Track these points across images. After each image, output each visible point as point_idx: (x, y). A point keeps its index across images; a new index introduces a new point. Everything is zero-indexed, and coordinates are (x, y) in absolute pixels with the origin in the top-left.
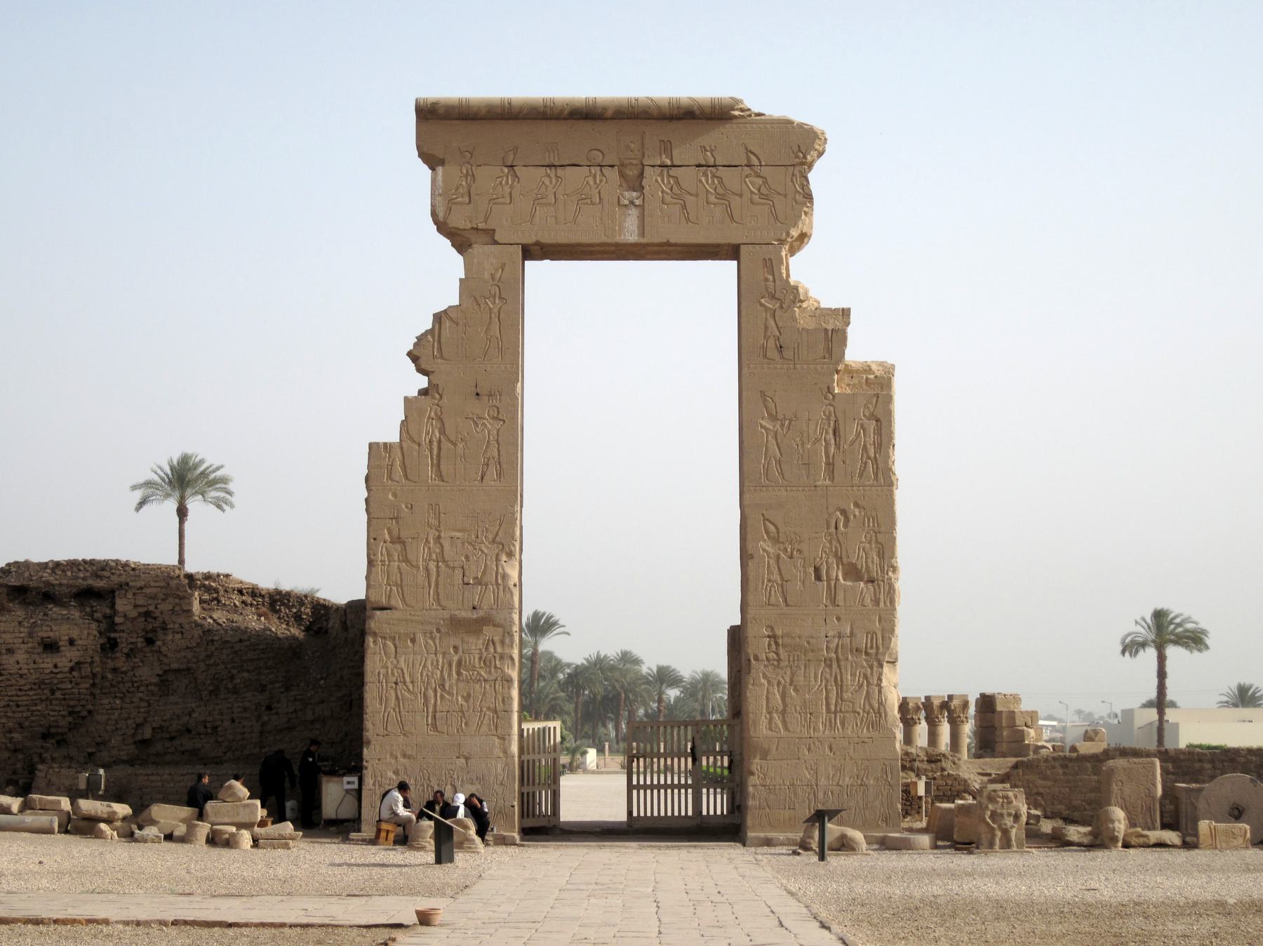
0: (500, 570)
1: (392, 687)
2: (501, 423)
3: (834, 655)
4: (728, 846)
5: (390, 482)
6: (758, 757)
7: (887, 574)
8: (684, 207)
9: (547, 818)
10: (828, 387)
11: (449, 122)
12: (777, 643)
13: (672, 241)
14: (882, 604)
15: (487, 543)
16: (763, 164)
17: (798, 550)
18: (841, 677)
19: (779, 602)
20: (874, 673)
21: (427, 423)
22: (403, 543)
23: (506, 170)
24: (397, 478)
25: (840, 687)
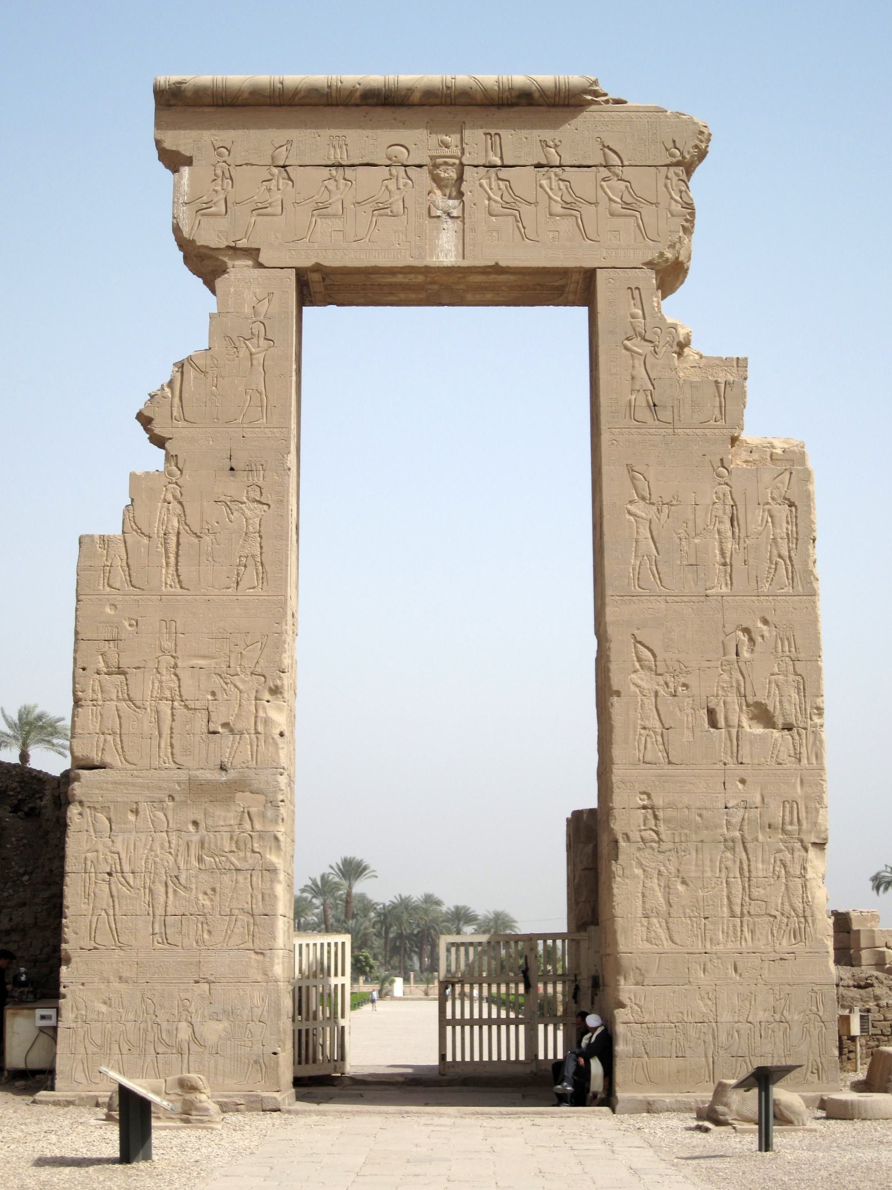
0: (261, 714)
1: (103, 880)
2: (266, 507)
3: (737, 834)
4: (590, 1113)
5: (108, 589)
6: (632, 980)
7: (811, 719)
8: (519, 220)
9: (332, 1064)
10: (722, 460)
11: (199, 110)
12: (656, 817)
13: (503, 264)
14: (804, 761)
15: (243, 676)
16: (626, 163)
17: (684, 685)
18: (749, 865)
19: (659, 758)
20: (796, 860)
21: (162, 507)
22: (124, 673)
23: (275, 171)
24: (118, 585)
25: (747, 876)
